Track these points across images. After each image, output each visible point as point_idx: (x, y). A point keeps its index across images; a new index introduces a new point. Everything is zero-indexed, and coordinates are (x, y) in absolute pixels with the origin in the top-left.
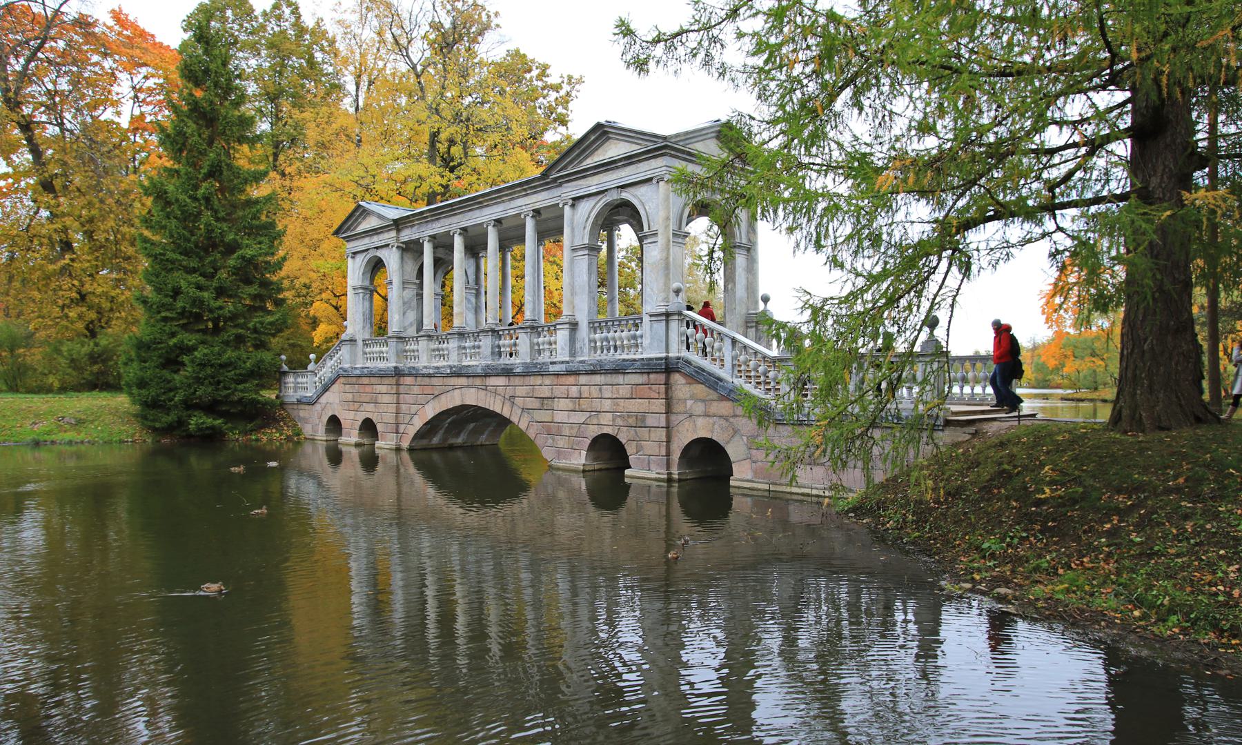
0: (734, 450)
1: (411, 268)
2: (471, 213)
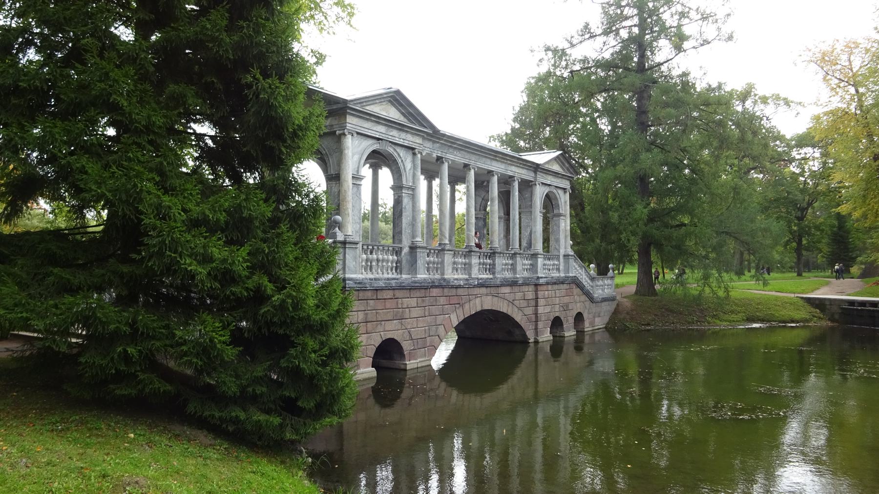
0: (585, 315)
2: (484, 159)
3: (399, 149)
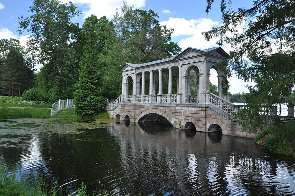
0: (223, 127)
1: (139, 79)
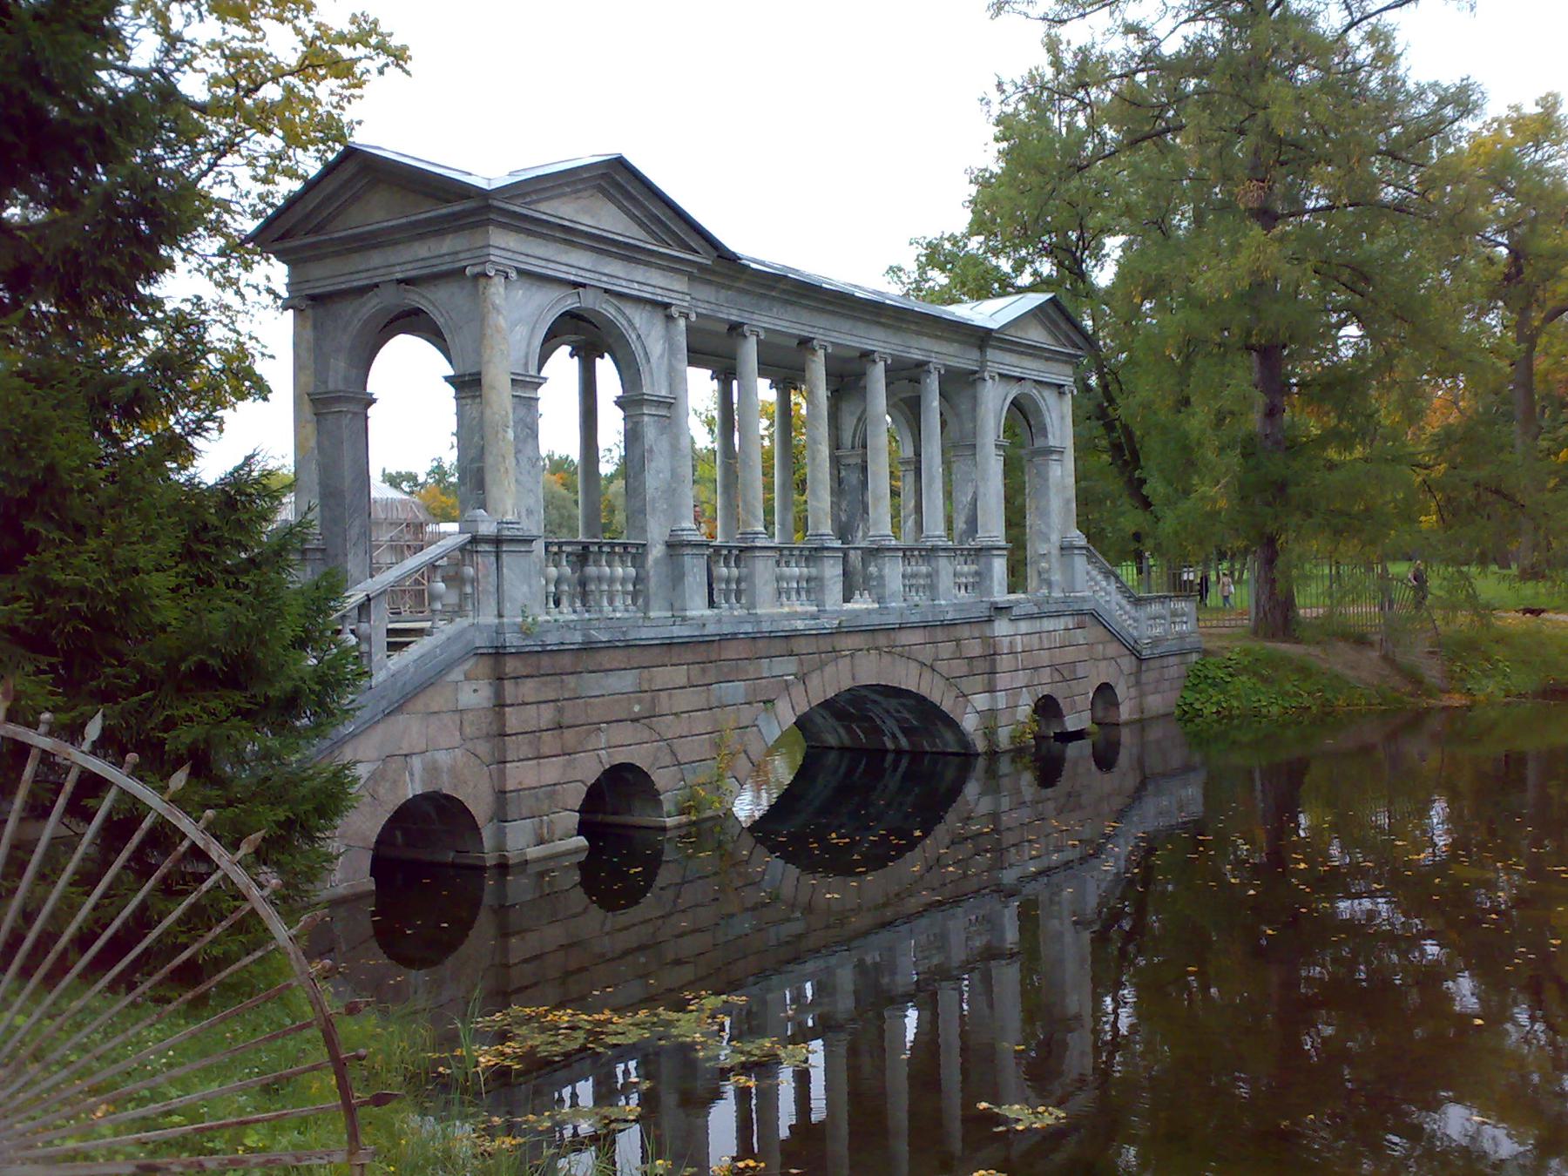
0: (1121, 691)
3: (632, 311)
